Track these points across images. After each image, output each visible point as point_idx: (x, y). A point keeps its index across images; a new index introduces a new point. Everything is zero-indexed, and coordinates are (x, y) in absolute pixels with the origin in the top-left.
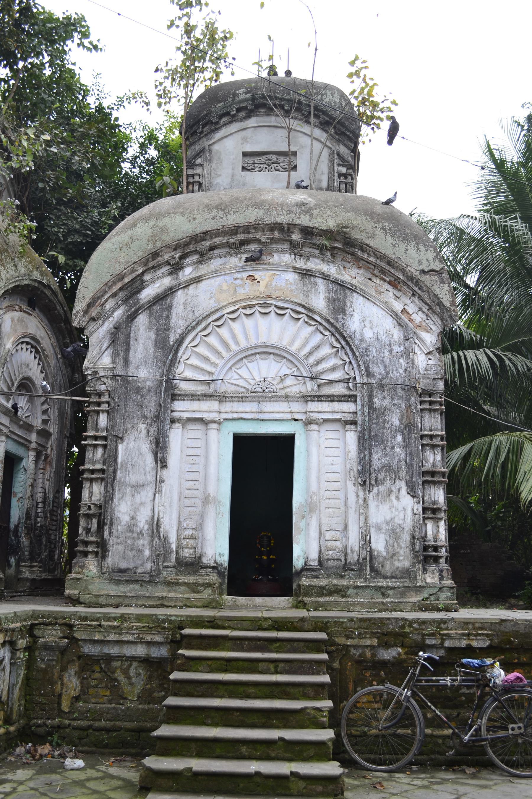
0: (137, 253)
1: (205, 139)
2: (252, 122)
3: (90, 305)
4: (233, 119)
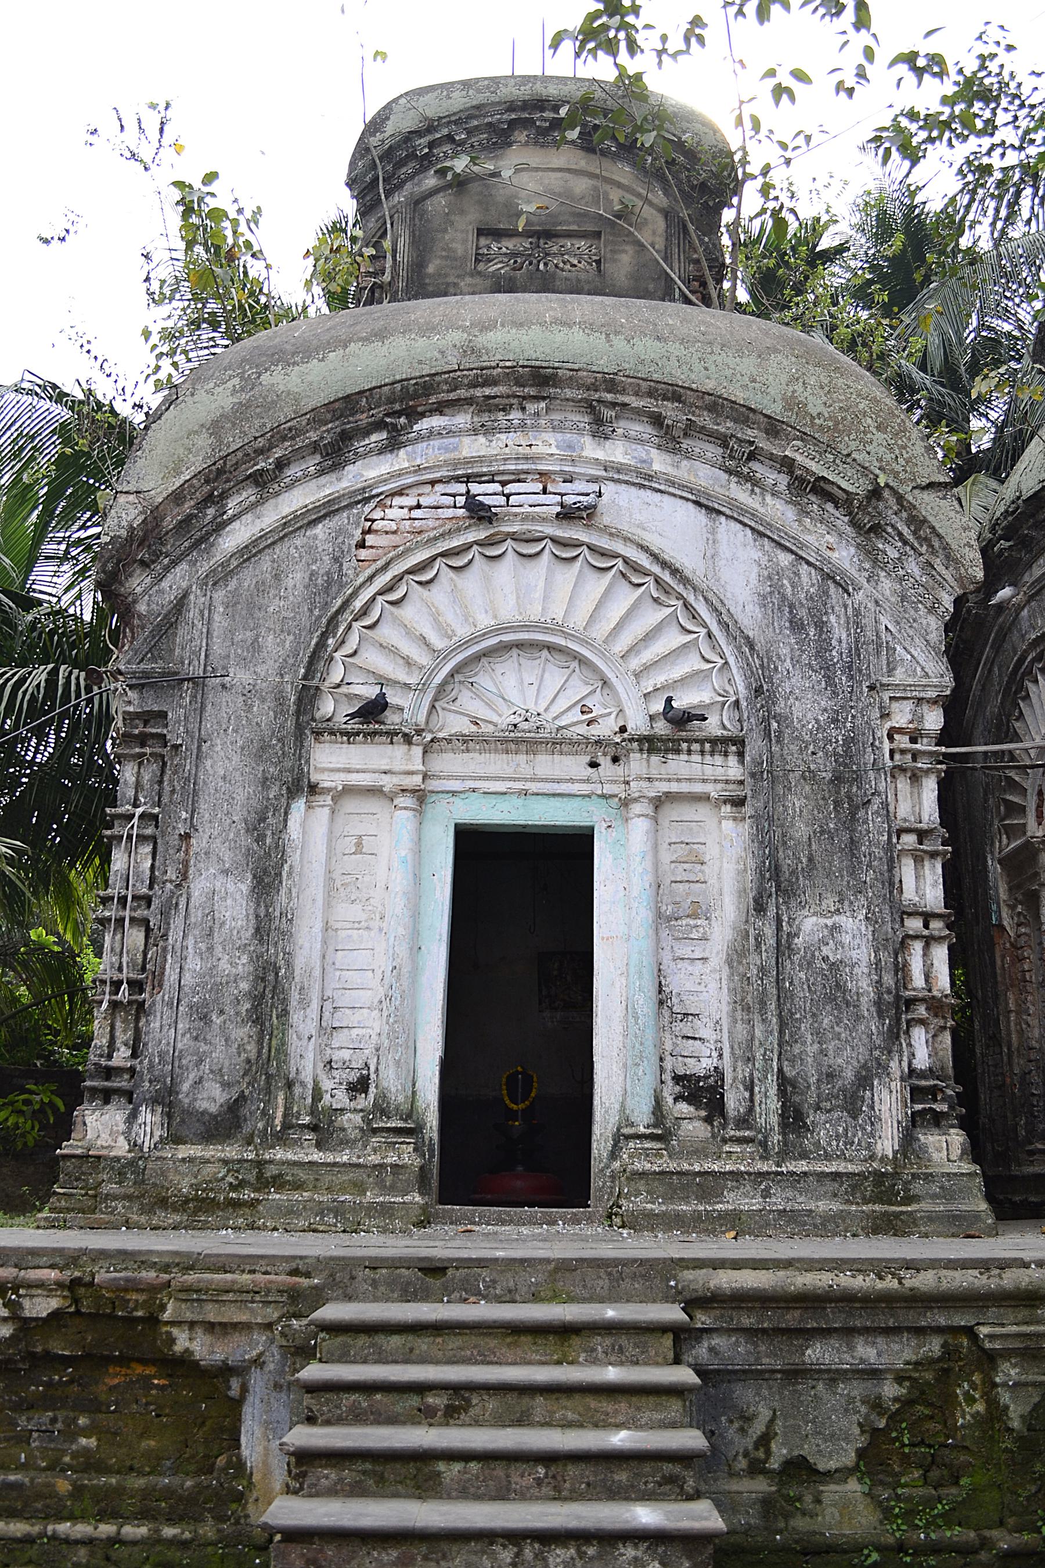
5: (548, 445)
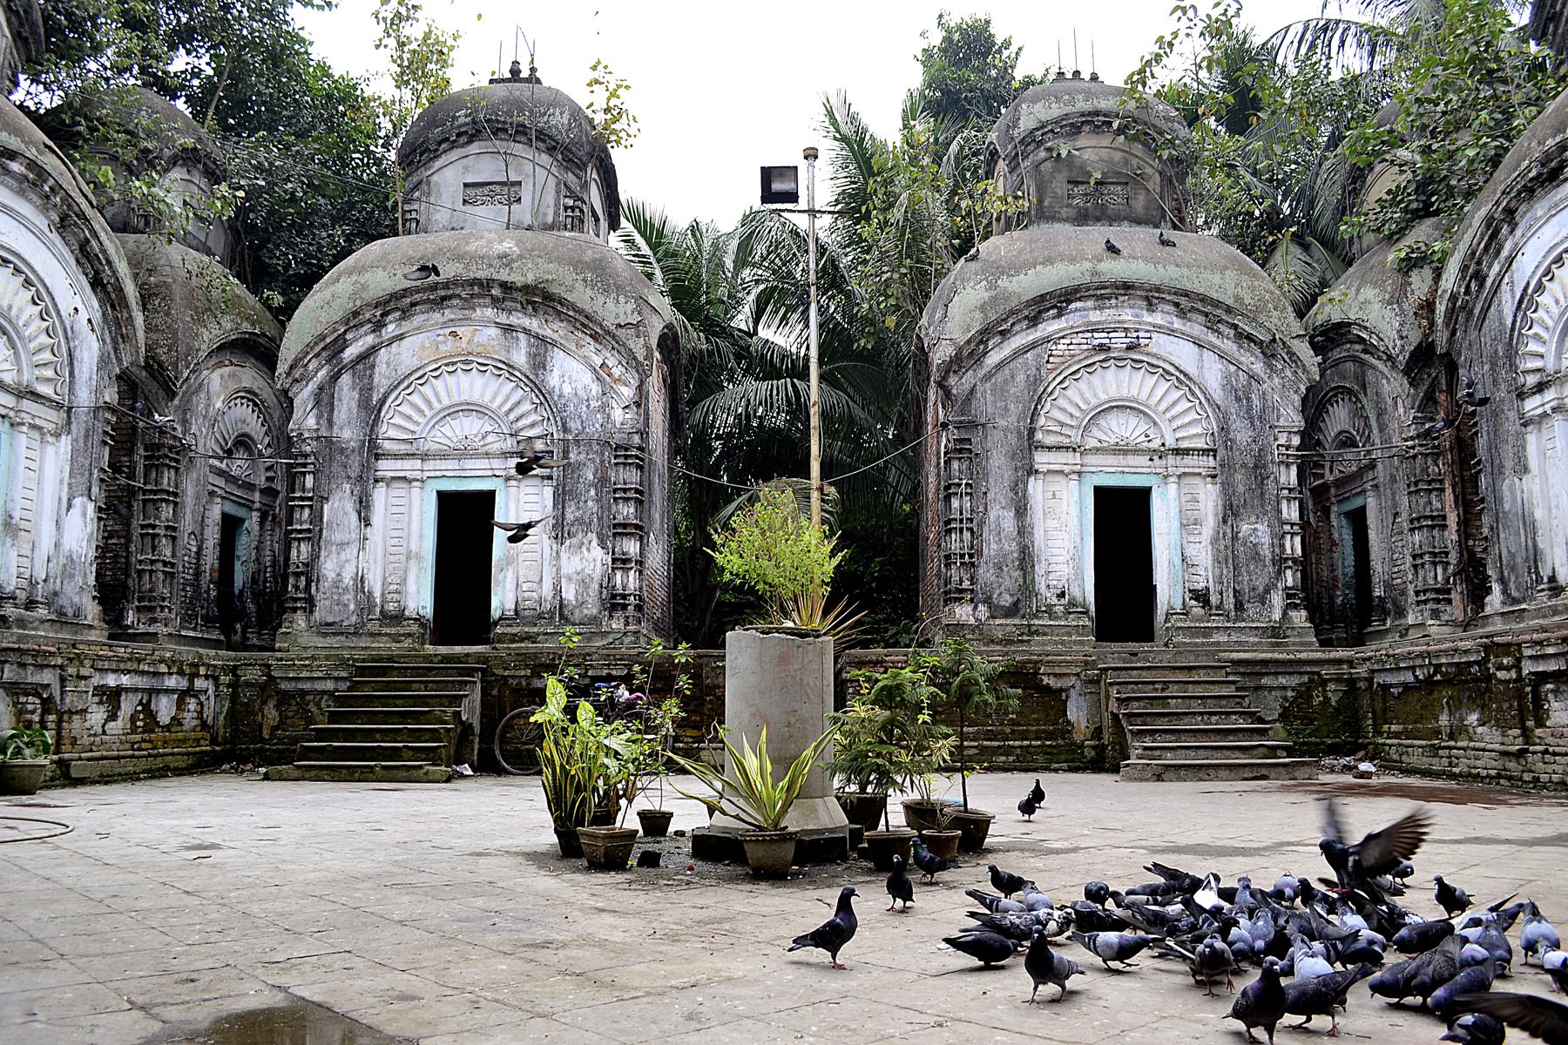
0: (337, 312)
2: (474, 148)
3: (291, 367)
4: (454, 145)
5: (1127, 315)
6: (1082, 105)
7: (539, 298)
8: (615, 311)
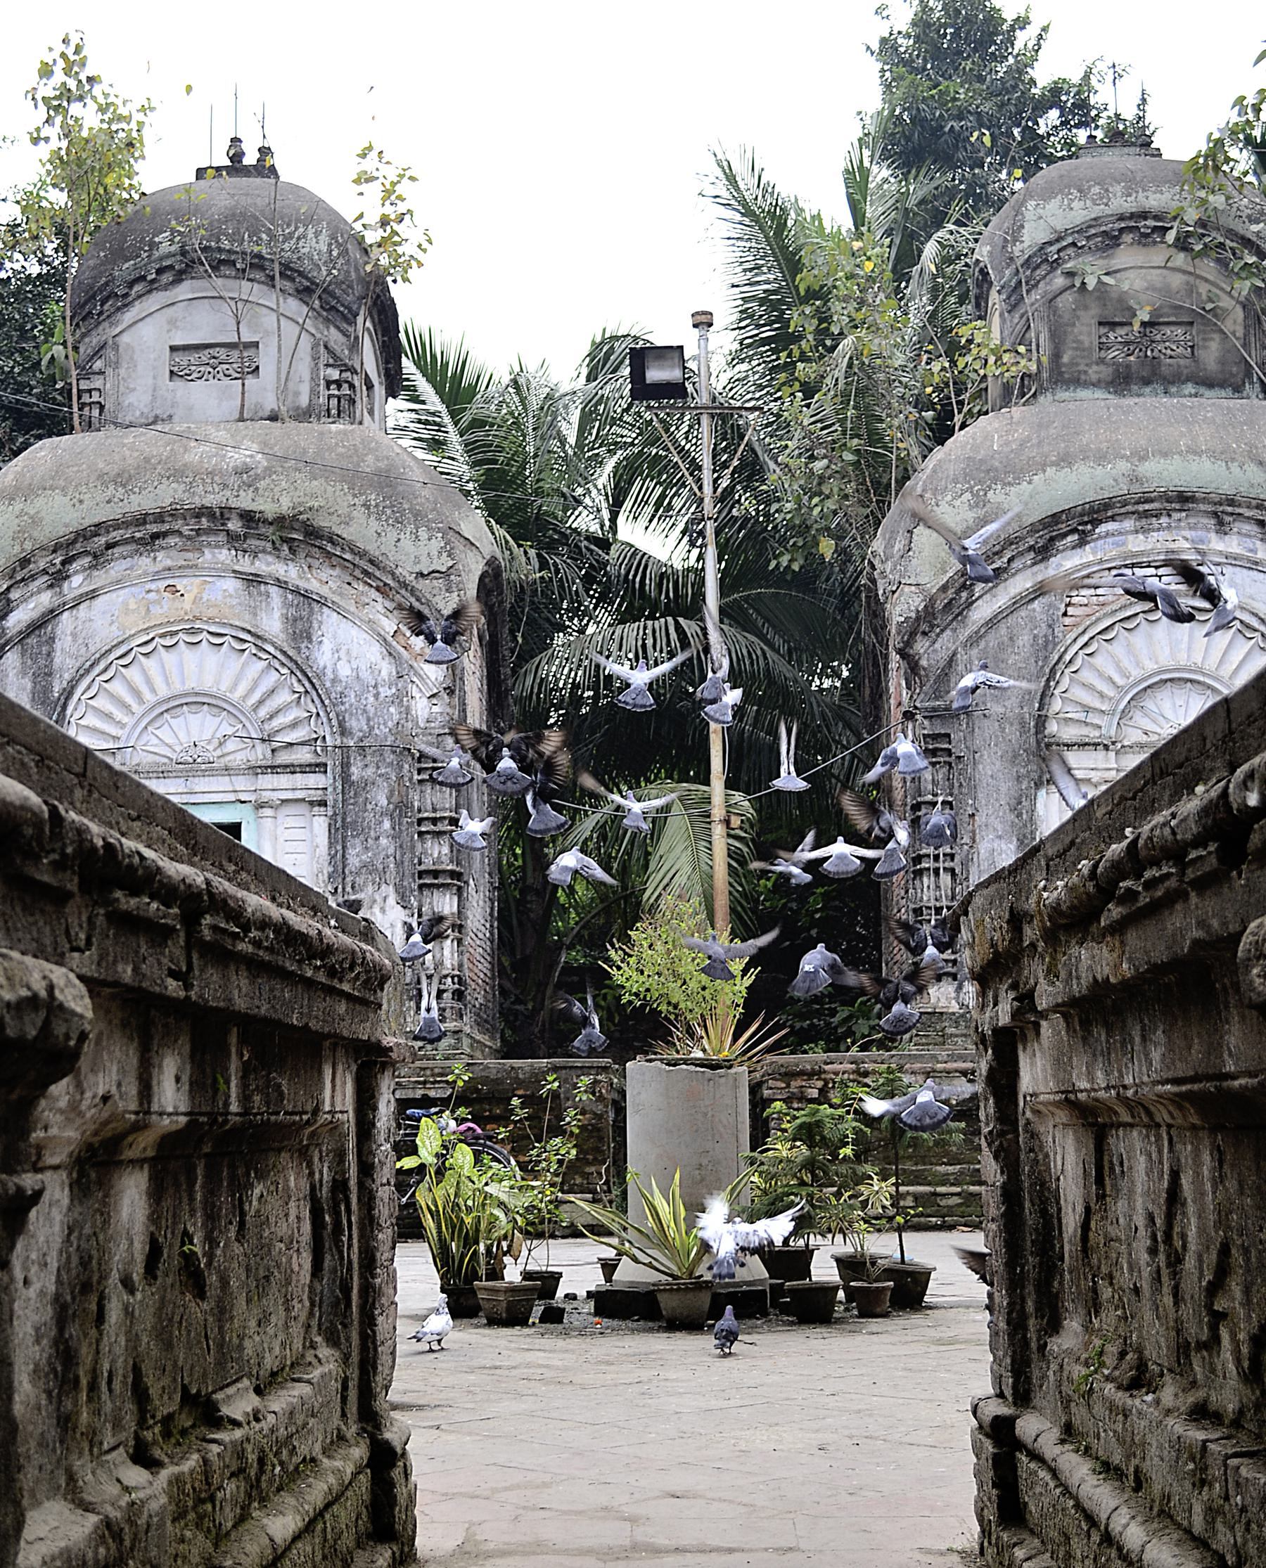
1: (106, 324)
2: (184, 290)
4: (153, 286)
6: (1121, 203)
7: (300, 535)
8: (412, 552)
